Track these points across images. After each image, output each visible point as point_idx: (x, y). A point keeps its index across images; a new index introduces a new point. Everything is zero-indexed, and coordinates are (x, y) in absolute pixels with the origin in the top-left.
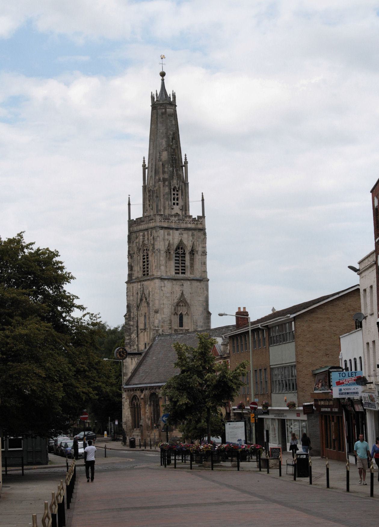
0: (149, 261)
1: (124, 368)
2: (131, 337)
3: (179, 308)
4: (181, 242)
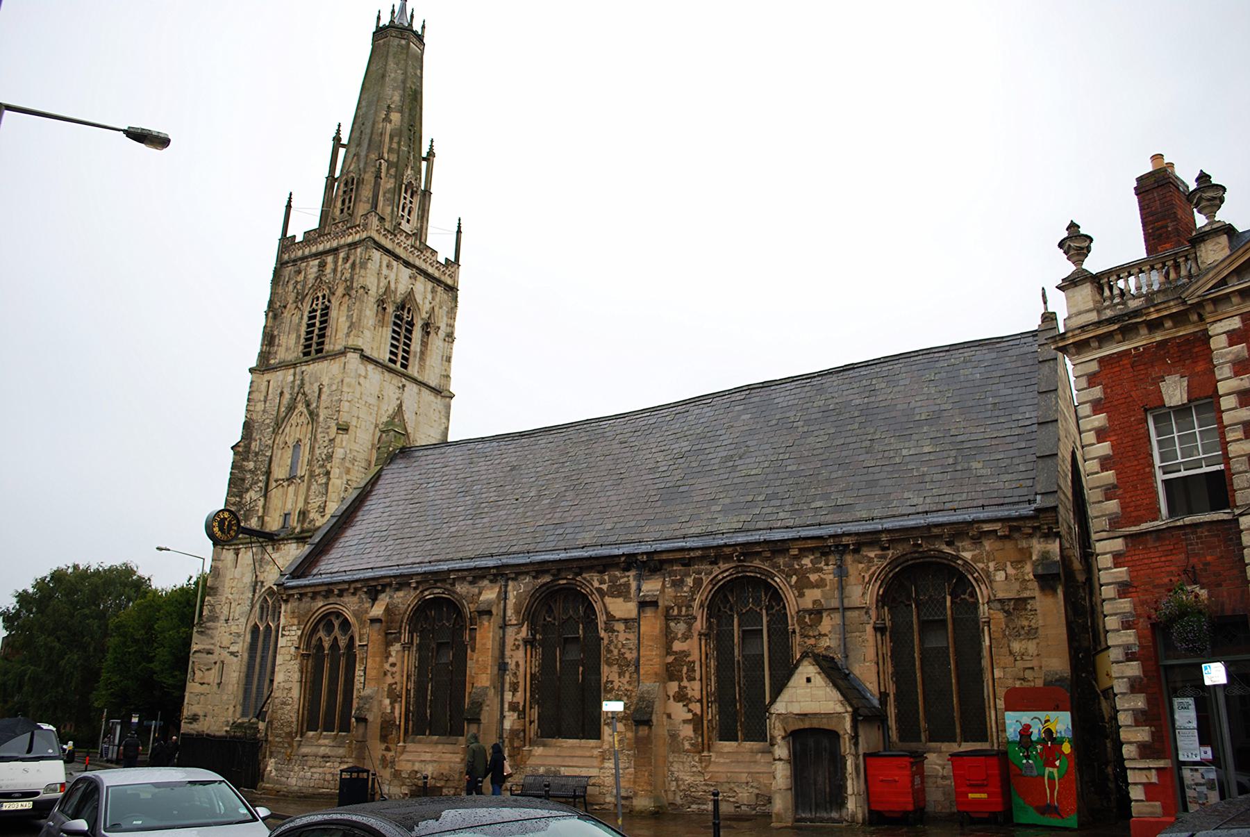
4: (410, 294)
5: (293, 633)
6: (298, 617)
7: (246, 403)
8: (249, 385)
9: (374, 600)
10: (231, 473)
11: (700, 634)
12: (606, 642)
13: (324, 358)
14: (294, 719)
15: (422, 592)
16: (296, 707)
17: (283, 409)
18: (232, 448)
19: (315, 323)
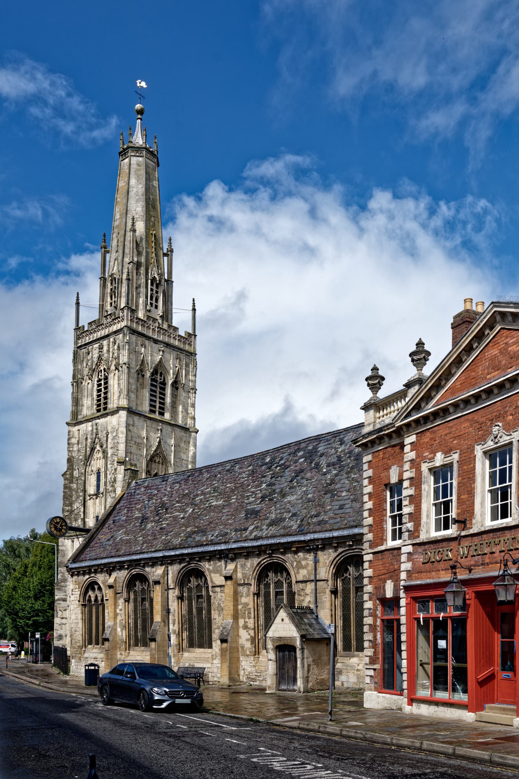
0: (109, 388)
1: (60, 555)
3: (154, 465)
5: (77, 593)
6: (78, 584)
7: (67, 446)
8: (67, 434)
9: (110, 575)
10: (64, 492)
11: (254, 594)
12: (212, 598)
14: (81, 639)
15: (131, 570)
16: (81, 632)
17: (88, 449)
18: (62, 475)
19: (101, 389)
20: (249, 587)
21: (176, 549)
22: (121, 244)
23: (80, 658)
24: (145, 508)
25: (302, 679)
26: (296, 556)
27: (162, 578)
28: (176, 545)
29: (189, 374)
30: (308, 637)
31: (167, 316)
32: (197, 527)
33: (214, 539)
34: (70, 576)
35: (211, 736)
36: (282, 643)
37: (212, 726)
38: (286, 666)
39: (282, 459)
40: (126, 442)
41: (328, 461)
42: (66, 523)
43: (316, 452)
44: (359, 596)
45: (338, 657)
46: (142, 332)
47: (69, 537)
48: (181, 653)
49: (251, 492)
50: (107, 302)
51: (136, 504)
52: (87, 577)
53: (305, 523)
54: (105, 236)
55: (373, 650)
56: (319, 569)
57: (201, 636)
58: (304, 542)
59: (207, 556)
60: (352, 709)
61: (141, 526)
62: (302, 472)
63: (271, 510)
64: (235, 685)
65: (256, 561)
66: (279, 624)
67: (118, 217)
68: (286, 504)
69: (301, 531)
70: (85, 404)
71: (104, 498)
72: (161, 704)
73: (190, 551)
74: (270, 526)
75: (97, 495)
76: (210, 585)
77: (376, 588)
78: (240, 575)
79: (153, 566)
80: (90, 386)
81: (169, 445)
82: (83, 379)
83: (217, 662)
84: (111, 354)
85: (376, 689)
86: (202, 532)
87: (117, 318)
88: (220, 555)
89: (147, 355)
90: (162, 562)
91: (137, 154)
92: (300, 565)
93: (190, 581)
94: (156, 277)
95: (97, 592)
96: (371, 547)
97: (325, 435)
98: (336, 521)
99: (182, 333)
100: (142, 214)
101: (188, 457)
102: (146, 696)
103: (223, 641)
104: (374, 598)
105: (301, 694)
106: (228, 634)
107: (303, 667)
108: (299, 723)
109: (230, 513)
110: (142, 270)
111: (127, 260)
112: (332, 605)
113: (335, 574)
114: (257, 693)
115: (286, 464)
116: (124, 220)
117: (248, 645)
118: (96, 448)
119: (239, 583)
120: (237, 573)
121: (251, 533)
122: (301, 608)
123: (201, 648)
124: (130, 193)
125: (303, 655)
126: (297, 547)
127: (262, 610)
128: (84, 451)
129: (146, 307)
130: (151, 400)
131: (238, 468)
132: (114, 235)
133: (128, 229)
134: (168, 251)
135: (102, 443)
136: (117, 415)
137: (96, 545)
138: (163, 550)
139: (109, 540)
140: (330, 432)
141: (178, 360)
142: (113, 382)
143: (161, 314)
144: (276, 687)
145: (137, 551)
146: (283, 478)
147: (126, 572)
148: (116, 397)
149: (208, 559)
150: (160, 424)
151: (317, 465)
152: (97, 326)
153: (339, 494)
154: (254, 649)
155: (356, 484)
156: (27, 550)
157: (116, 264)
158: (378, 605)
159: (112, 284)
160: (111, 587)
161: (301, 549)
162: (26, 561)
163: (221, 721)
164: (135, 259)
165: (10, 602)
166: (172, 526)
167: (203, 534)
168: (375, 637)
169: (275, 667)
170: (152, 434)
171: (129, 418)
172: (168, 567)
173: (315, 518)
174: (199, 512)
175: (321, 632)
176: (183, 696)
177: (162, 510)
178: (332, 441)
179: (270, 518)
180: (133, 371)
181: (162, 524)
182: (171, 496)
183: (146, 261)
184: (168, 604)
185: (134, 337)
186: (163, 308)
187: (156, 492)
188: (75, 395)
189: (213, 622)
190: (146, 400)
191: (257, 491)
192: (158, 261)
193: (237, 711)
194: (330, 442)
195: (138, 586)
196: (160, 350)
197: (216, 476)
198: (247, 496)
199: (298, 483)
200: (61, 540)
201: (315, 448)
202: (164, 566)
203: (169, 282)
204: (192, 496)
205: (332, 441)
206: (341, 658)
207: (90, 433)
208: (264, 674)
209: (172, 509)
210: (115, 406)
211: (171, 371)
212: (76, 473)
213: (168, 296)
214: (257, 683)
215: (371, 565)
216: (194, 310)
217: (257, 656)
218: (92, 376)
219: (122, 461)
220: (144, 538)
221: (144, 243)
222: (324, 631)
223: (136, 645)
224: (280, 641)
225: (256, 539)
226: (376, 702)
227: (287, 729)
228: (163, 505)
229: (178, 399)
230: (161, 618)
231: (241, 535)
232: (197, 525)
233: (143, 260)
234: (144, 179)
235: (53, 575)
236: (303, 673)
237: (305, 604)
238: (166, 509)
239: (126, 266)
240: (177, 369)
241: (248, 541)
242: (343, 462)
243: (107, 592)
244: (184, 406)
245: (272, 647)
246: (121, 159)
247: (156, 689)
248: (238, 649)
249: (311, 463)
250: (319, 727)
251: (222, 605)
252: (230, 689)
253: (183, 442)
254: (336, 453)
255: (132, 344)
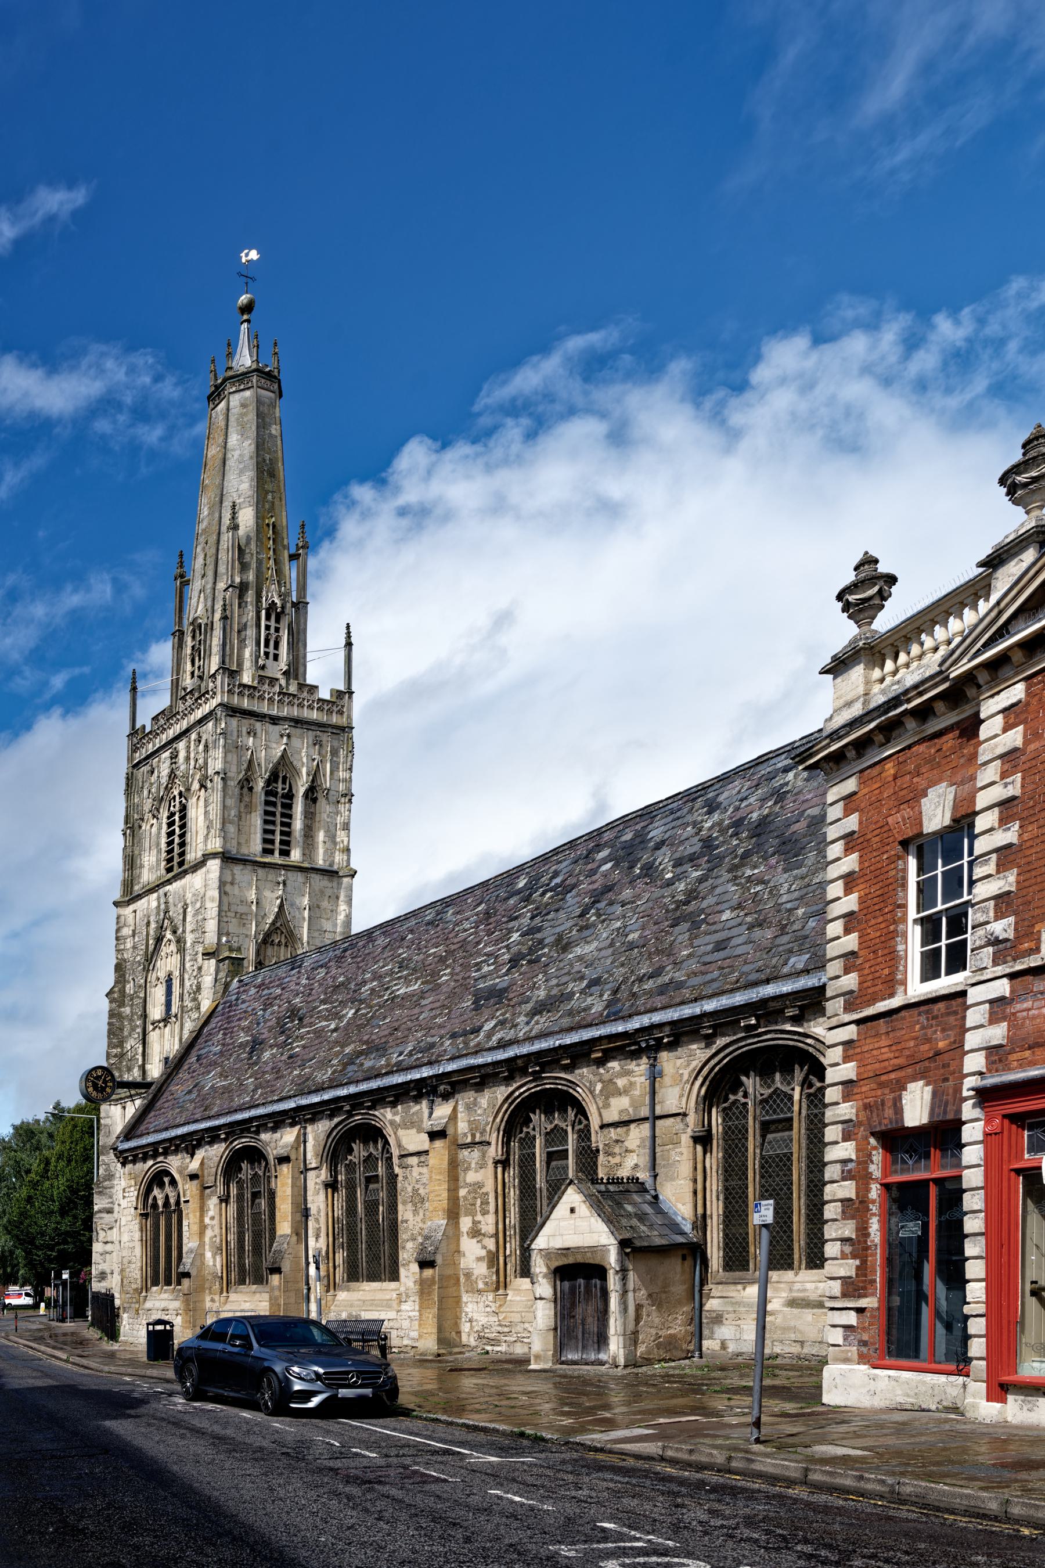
0: (189, 824)
1: (102, 1133)
2: (122, 1047)
3: (270, 951)
13: (185, 872)
20: (485, 1148)
21: (323, 1089)
22: (210, 561)
23: (137, 1311)
24: (258, 1024)
25: (621, 1338)
26: (601, 1070)
27: (294, 1151)
28: (323, 1083)
29: (338, 768)
30: (638, 1243)
31: (296, 669)
32: (366, 1042)
33: (403, 1060)
34: (119, 1165)
35: (445, 1481)
36: (570, 1260)
37: (436, 1452)
38: (579, 1311)
39: (556, 874)
40: (219, 915)
41: (677, 855)
42: (113, 1076)
43: (641, 842)
44: (770, 1143)
45: (710, 1286)
46: (250, 708)
47: (117, 1100)
48: (332, 1292)
49: (486, 954)
50: (185, 672)
51: (240, 1019)
52: (150, 1163)
53: (623, 995)
54: (181, 555)
55: (857, 1262)
56: (663, 1090)
57: (374, 1257)
58: (625, 1035)
59: (389, 1096)
60: (790, 1407)
61: (251, 1058)
62: (610, 890)
63: (536, 983)
64: (451, 1354)
65: (501, 1092)
66: (563, 1219)
67: (206, 513)
68: (571, 965)
69: (615, 1014)
70: (146, 864)
71: (178, 1023)
72: (309, 1400)
73: (352, 1089)
74: (535, 1014)
75: (166, 1020)
76: (395, 1152)
77: (867, 1107)
78: (462, 1126)
79: (274, 1129)
80: (154, 829)
81: (299, 909)
82: (142, 820)
83: (410, 1307)
84: (192, 763)
85: (862, 1359)
86: (377, 1050)
87: (203, 695)
88: (420, 1091)
89: (258, 749)
90: (293, 1118)
91: (242, 387)
92: (611, 1087)
93: (351, 1151)
94: (277, 600)
95: (168, 1189)
96: (848, 1008)
97: (665, 803)
98: (709, 977)
99: (324, 694)
100: (250, 493)
101: (336, 925)
102: (275, 1383)
103: (425, 1264)
104: (862, 1131)
105: (619, 1372)
106: (437, 1249)
107: (625, 1310)
108: (664, 1448)
109: (438, 1004)
110: (250, 596)
111: (221, 585)
112: (695, 1169)
113: (705, 1097)
114: (509, 1371)
115: (568, 882)
116: (217, 515)
117: (481, 1270)
118: (164, 936)
119: (460, 1142)
120: (456, 1123)
121: (489, 1035)
122: (618, 1181)
123: (374, 1281)
124: (227, 463)
125: (625, 1285)
126: (603, 1051)
127: (513, 1195)
128: (143, 947)
129: (257, 662)
130: (265, 831)
131: (453, 914)
132: (199, 549)
133: (224, 529)
134: (298, 549)
135: (175, 926)
136: (204, 869)
137: (166, 1105)
138: (295, 1096)
139: (190, 1092)
140: (679, 793)
141: (317, 747)
142: (196, 814)
143: (285, 668)
144: (553, 1356)
145: (244, 1104)
146: (561, 912)
147: (224, 1145)
148: (201, 838)
149: (390, 1102)
150: (283, 872)
151: (649, 870)
152: (168, 720)
153: (711, 919)
154: (494, 1278)
155: (758, 888)
156: (51, 1136)
157: (202, 599)
158: (875, 1148)
159: (194, 637)
160: (193, 1177)
161: (614, 1054)
162: (46, 1153)
163: (450, 1438)
164: (238, 580)
165: (21, 1223)
166: (313, 1048)
167: (379, 1053)
168: (863, 1230)
169: (552, 1312)
170: (267, 893)
171: (225, 871)
172: (305, 1128)
173: (651, 981)
174: (368, 1013)
175: (667, 1231)
176: (356, 1382)
177: (293, 1021)
178: (685, 810)
179: (534, 999)
180: (232, 783)
181: (292, 1049)
182: (310, 994)
183: (257, 577)
184: (305, 1200)
185: (234, 722)
186: (288, 657)
187: (279, 991)
188: (129, 850)
189: (401, 1227)
190: (255, 833)
191: (499, 950)
192: (279, 572)
193: (461, 1410)
194: (678, 814)
195: (246, 1170)
196: (282, 736)
197: (403, 939)
198: (477, 964)
199: (599, 915)
200: (104, 1107)
201: (641, 838)
202: (298, 1127)
203: (301, 605)
204: (352, 986)
205: (685, 810)
206: (720, 1287)
207: (155, 912)
208: (519, 1328)
209: (311, 1017)
210: (200, 854)
211: (304, 770)
212: (130, 988)
213: (298, 633)
214: (503, 1348)
215: (851, 1052)
216: (349, 645)
217: (501, 1292)
218: (159, 811)
219: (211, 951)
220: (256, 1079)
221: (253, 546)
222: (674, 1227)
223: (242, 1281)
224: (565, 1255)
225: (503, 1045)
226: (864, 1390)
227: (631, 1462)
228: (294, 1013)
229: (317, 819)
230: (292, 1227)
231: (466, 1043)
232: (365, 1038)
233: (251, 576)
234: (254, 428)
235: (91, 1172)
236: (625, 1324)
237: (624, 1173)
238: (301, 1019)
239: (219, 596)
240: (315, 763)
241: (485, 1053)
242: (717, 848)
243: (187, 1187)
244: (327, 831)
245: (544, 1270)
246: (212, 406)
247: (296, 1369)
248: (458, 1280)
249: (631, 867)
250: (730, 1459)
251: (422, 1191)
252: (440, 1361)
253: (327, 898)
254: (697, 834)
255: (231, 735)
